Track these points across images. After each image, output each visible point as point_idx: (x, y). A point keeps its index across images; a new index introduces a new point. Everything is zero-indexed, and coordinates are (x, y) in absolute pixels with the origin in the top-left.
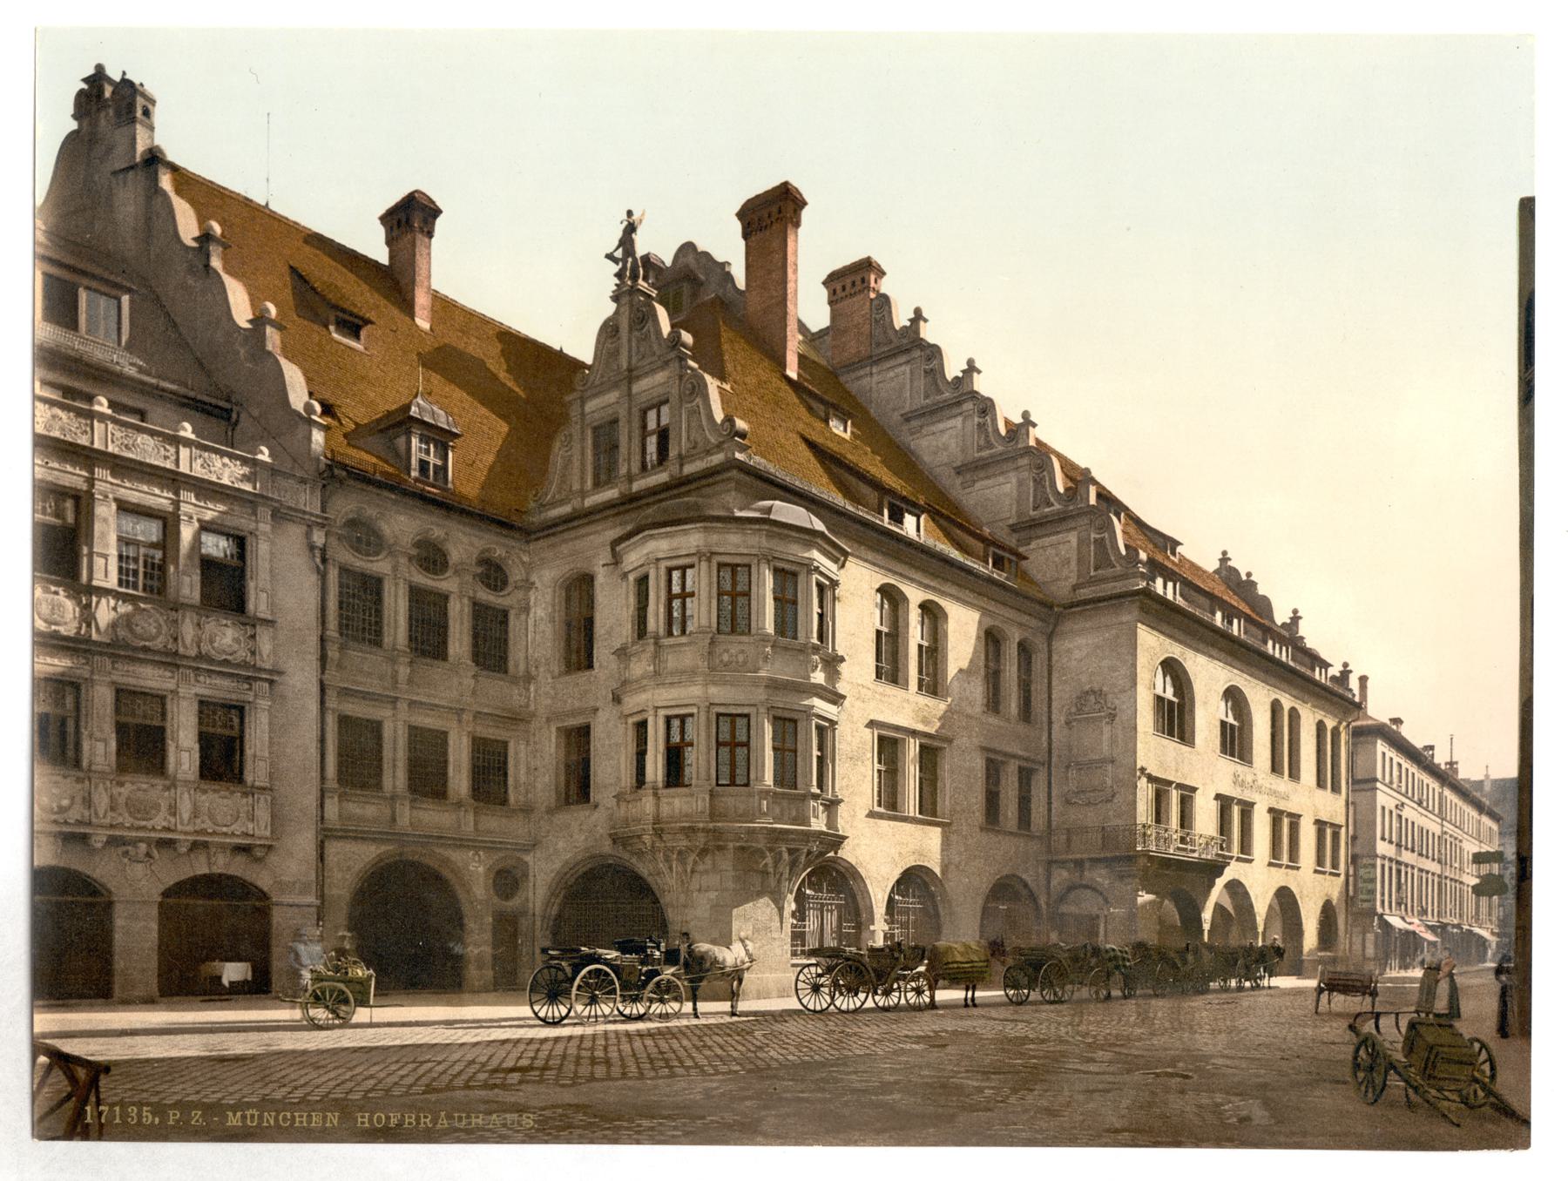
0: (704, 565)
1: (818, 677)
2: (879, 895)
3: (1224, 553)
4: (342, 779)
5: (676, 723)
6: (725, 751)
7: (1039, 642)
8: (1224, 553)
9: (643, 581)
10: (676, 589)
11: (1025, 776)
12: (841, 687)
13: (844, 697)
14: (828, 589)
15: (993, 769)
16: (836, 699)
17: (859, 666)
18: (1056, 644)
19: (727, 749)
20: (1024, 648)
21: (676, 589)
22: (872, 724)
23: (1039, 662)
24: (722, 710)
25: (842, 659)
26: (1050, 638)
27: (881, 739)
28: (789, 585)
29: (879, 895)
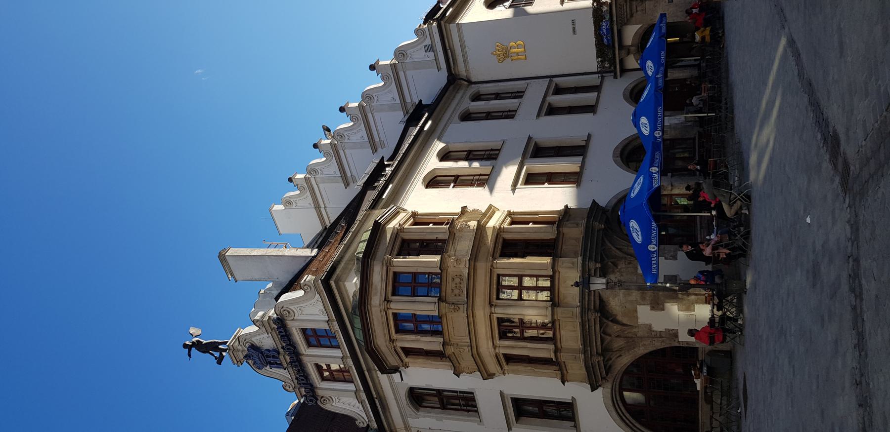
0: (392, 306)
1: (473, 224)
6: (525, 295)
7: (474, 89)
9: (408, 352)
10: (410, 326)
11: (559, 91)
12: (483, 211)
13: (490, 206)
14: (417, 219)
15: (552, 111)
16: (491, 211)
17: (474, 198)
19: (524, 293)
20: (477, 97)
21: (410, 326)
23: (485, 89)
24: (495, 297)
26: (470, 82)
28: (413, 246)
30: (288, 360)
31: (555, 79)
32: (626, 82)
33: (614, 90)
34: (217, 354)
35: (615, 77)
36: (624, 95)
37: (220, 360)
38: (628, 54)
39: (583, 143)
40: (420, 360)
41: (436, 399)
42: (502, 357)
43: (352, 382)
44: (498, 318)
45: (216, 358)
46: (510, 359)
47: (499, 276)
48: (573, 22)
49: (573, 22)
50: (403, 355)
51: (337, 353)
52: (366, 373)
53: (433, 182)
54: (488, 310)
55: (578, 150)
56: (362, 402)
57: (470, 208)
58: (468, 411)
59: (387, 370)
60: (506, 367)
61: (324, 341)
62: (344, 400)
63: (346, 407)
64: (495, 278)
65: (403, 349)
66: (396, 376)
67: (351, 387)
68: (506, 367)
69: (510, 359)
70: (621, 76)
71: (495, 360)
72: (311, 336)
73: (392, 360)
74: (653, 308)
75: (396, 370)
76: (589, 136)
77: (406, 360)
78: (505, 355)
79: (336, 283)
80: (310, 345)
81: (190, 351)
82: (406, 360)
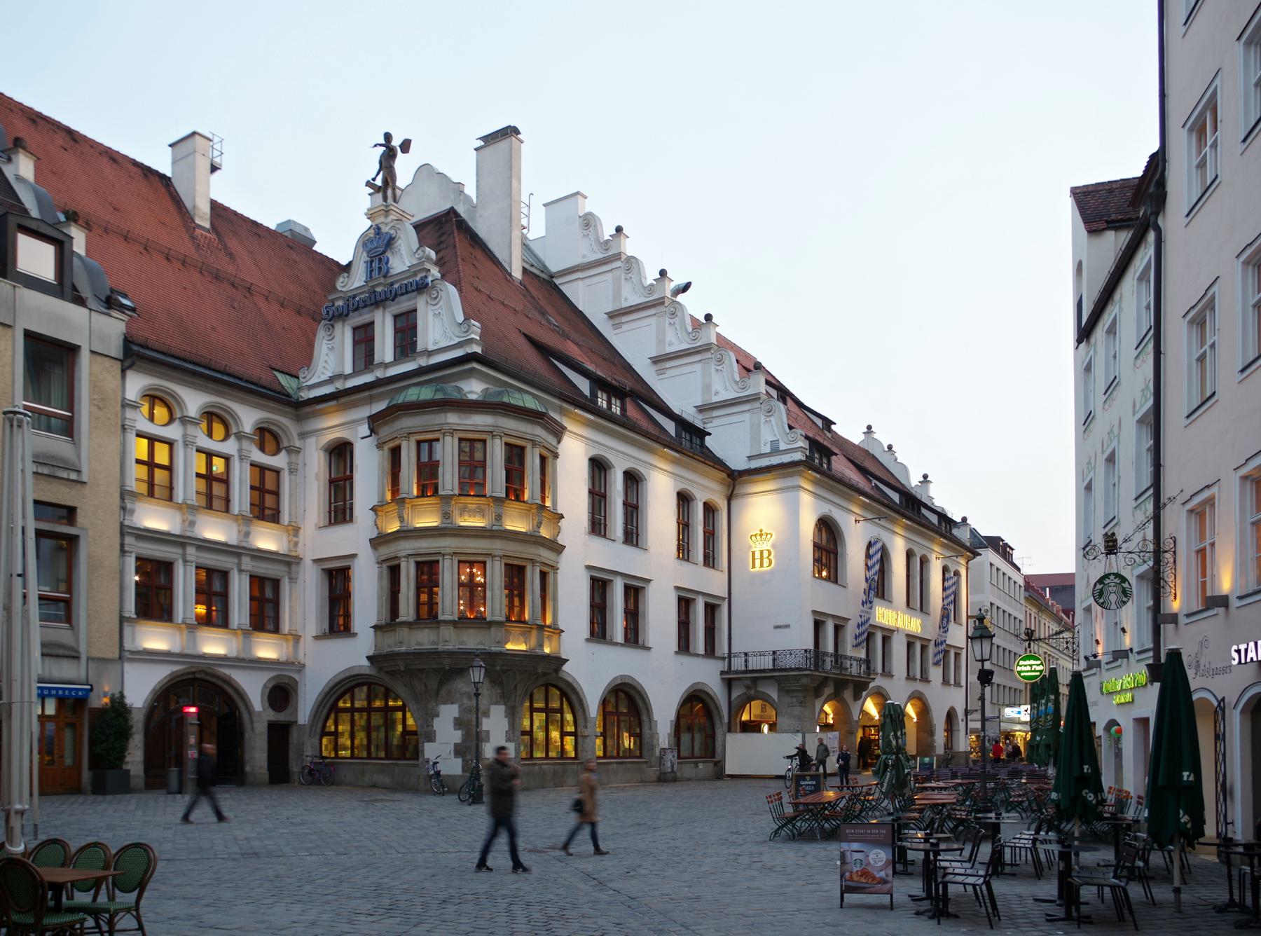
2: (593, 708)
3: (869, 427)
4: (41, 794)
8: (869, 427)
9: (395, 453)
10: (425, 458)
12: (561, 540)
15: (685, 603)
16: (559, 549)
22: (589, 567)
24: (462, 558)
25: (562, 517)
27: (593, 579)
29: (593, 708)
30: (379, 289)
32: (715, 687)
33: (707, 674)
35: (722, 673)
38: (748, 688)
39: (640, 641)
40: (387, 465)
41: (341, 475)
42: (396, 562)
44: (438, 562)
46: (394, 571)
47: (484, 563)
48: (787, 626)
49: (787, 626)
50: (391, 445)
52: (367, 394)
53: (598, 466)
54: (448, 551)
55: (634, 637)
56: (331, 380)
57: (563, 523)
59: (375, 422)
62: (332, 357)
63: (323, 357)
64: (481, 559)
66: (364, 429)
68: (385, 566)
69: (394, 571)
70: (723, 679)
71: (393, 555)
73: (385, 432)
75: (373, 431)
76: (649, 649)
77: (386, 448)
82: (386, 448)
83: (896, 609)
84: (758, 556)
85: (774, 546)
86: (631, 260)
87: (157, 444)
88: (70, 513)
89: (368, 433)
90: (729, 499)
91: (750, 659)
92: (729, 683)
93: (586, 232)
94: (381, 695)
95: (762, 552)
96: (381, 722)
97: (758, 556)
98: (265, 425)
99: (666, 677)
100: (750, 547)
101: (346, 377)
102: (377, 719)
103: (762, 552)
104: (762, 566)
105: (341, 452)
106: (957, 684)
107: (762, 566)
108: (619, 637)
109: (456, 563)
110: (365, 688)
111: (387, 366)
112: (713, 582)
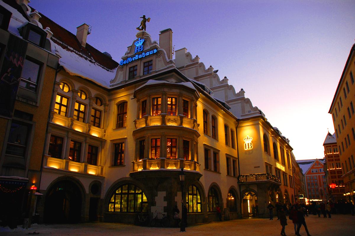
5: (154, 141)
11: (234, 161)
18: (238, 129)
31: (237, 160)
34: (140, 28)
36: (233, 186)
37: (138, 29)
42: (144, 139)
43: (129, 79)
45: (139, 27)
48: (259, 167)
49: (259, 167)
51: (142, 74)
52: (134, 85)
56: (121, 83)
58: (117, 125)
60: (138, 140)
61: (146, 69)
65: (146, 101)
67: (127, 79)
72: (149, 63)
74: (164, 197)
78: (144, 140)
79: (173, 75)
80: (144, 63)
81: (143, 18)
83: (280, 164)
84: (247, 145)
85: (252, 142)
86: (202, 63)
87: (63, 98)
88: (31, 116)
89: (133, 98)
90: (236, 128)
91: (248, 178)
92: (240, 186)
93: (187, 58)
94: (133, 188)
95: (248, 144)
96: (133, 198)
97: (247, 145)
98: (98, 96)
99: (225, 183)
100: (244, 142)
101: (126, 81)
102: (131, 197)
103: (248, 144)
104: (249, 148)
105: (122, 106)
106: (292, 187)
107: (249, 148)
108: (213, 170)
109: (166, 139)
110: (127, 186)
111: (141, 77)
112: (234, 153)
